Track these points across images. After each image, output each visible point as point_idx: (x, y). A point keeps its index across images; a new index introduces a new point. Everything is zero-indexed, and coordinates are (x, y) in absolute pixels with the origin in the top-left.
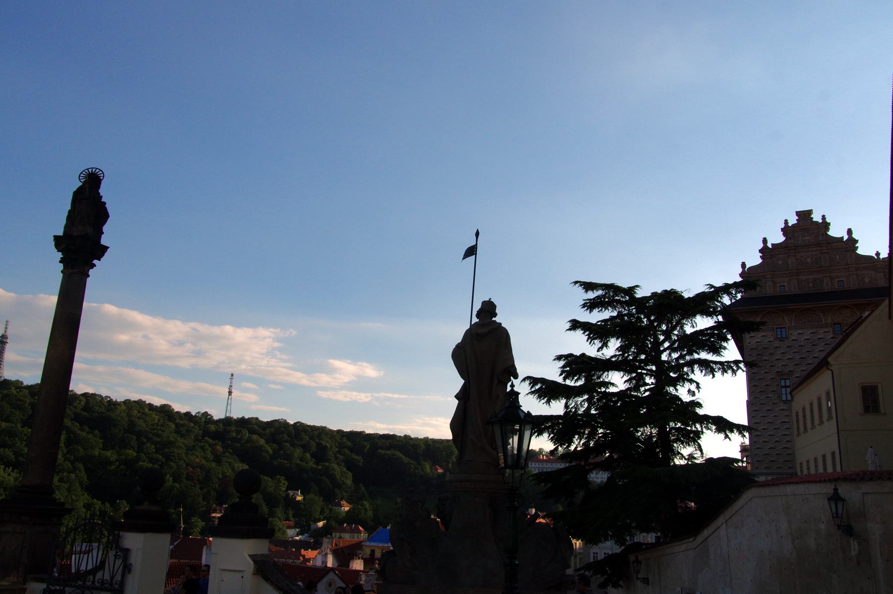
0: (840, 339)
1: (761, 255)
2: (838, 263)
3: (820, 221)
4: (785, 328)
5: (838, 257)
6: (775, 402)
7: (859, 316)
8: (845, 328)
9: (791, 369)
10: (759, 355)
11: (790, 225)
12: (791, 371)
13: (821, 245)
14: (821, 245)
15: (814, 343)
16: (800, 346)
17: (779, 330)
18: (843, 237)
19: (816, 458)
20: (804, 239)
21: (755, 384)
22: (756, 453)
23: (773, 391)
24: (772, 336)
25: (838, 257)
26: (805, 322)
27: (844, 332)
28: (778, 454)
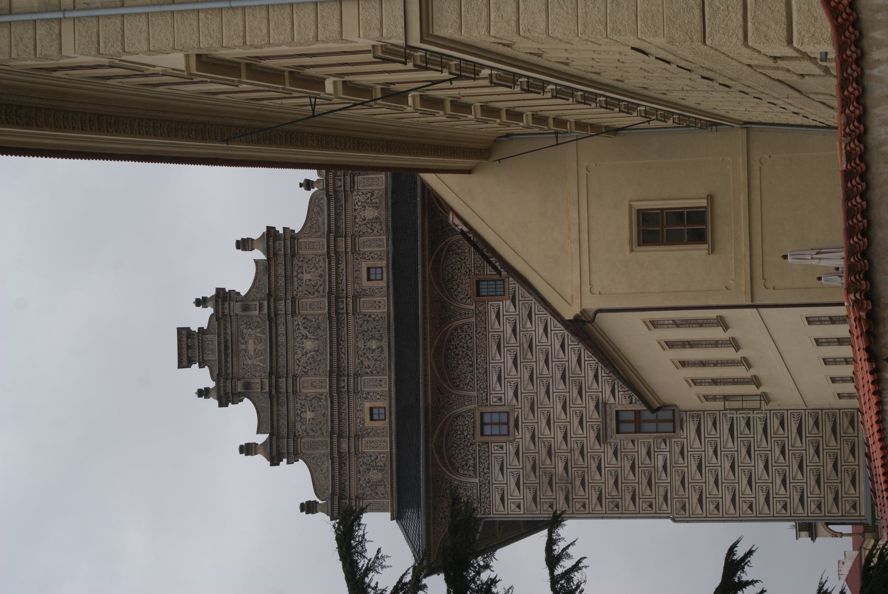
0: (517, 286)
1: (285, 460)
3: (210, 311)
4: (482, 414)
5: (306, 276)
6: (678, 450)
7: (460, 237)
8: (489, 270)
9: (592, 405)
10: (550, 483)
11: (212, 384)
12: (597, 407)
13: (272, 315)
14: (272, 315)
15: (526, 346)
16: (531, 378)
17: (487, 430)
18: (257, 262)
19: (826, 361)
20: (252, 353)
21: (628, 497)
22: (813, 507)
23: (649, 453)
24: (502, 447)
25: (306, 276)
26: (471, 366)
27: (499, 273)
28: (817, 452)
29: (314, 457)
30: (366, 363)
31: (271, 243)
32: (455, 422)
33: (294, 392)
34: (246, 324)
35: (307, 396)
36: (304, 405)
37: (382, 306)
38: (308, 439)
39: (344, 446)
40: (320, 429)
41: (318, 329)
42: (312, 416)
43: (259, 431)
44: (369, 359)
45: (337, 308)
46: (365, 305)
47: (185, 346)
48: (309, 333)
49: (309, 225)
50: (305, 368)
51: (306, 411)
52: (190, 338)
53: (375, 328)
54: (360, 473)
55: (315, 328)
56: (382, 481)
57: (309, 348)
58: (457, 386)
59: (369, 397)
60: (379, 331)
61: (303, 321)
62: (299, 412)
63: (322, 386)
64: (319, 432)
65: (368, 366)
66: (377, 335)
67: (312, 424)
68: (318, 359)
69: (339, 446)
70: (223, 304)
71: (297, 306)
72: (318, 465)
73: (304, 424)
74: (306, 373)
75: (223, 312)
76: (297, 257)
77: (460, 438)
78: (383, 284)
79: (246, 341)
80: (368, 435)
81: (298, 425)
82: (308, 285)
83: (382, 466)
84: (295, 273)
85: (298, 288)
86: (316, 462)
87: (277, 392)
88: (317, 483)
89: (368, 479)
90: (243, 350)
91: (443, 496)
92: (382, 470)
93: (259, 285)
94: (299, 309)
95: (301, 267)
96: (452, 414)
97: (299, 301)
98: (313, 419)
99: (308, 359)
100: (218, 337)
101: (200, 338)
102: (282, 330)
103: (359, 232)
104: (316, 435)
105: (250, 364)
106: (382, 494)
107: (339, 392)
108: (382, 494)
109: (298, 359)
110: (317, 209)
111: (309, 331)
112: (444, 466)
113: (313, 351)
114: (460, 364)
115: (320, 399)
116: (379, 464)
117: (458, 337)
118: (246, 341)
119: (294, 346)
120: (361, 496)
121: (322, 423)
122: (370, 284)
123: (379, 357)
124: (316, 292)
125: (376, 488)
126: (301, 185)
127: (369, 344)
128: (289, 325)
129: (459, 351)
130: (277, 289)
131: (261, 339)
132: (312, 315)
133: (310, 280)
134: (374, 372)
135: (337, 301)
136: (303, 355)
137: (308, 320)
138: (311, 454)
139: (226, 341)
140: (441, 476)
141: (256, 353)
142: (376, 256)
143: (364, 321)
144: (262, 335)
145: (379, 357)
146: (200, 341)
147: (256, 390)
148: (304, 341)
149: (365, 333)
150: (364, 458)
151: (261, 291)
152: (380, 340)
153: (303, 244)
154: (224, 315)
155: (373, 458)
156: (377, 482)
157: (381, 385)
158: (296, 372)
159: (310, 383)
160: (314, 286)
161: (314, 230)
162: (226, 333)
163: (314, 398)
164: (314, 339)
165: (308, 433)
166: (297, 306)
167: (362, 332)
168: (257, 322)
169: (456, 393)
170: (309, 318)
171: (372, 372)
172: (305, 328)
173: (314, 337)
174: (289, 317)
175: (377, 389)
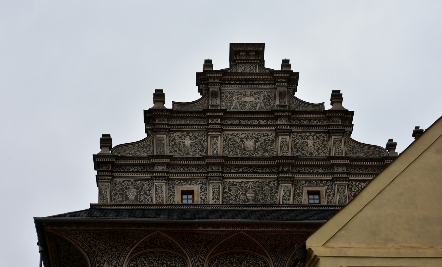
2: (311, 154)
18: (322, 104)
20: (243, 99)
25: (310, 143)
29: (150, 145)
30: (233, 188)
31: (340, 115)
32: (179, 259)
33: (207, 131)
34: (268, 95)
35: (204, 141)
36: (196, 138)
37: (285, 202)
38: (166, 140)
39: (160, 168)
42: (186, 144)
43: (174, 103)
44: (237, 191)
45: (283, 165)
46: (286, 188)
48: (260, 144)
49: (356, 146)
50: (230, 140)
51: (191, 140)
53: (265, 196)
54: (135, 181)
55: (265, 148)
56: (127, 199)
58: (212, 262)
59: (203, 190)
60: (263, 199)
61: (271, 139)
62: (191, 134)
63: (213, 152)
64: (172, 150)
65: (231, 190)
67: (180, 144)
68: (237, 150)
69: (159, 164)
70: (285, 78)
71: (284, 134)
72: (143, 148)
74: (225, 140)
76: (328, 136)
77: (163, 263)
78: (305, 202)
79: (253, 95)
80: (168, 189)
81: (179, 134)
82: (303, 143)
83: (140, 199)
84: (313, 134)
85: (300, 136)
87: (209, 117)
88: (127, 147)
89: (129, 188)
90: (245, 93)
91: (110, 245)
92: (136, 199)
93: (302, 107)
95: (319, 138)
96: (186, 257)
97: (288, 135)
98: (184, 145)
99: (237, 143)
100: (257, 73)
101: (255, 61)
102: (263, 122)
103: (351, 185)
105: (234, 98)
106: (114, 199)
107: (208, 165)
108: (114, 199)
109: (237, 134)
110: (370, 152)
111: (262, 143)
112: (138, 246)
113: (244, 147)
114: (232, 265)
115: (202, 151)
116: (142, 197)
117: (258, 264)
118: (253, 95)
119: (249, 132)
120: (114, 181)
121: (180, 152)
122: (305, 193)
123: (240, 199)
124: (297, 149)
125: (120, 194)
126: (391, 140)
127: (251, 191)
128: (268, 128)
129: (245, 265)
130: (299, 119)
132: (276, 147)
133: (307, 145)
134: (225, 195)
136: (241, 138)
138: (153, 143)
139: (252, 80)
140: (129, 242)
141: (243, 103)
142: (331, 198)
143: (271, 187)
144: (258, 107)
145: (240, 199)
146: (253, 61)
147: (210, 101)
148: (254, 140)
149: (261, 187)
150: (148, 185)
151: (297, 108)
152: (254, 201)
154: (275, 78)
155: (148, 192)
156: (126, 195)
157: (213, 199)
158: (226, 133)
160: (302, 149)
161: (351, 149)
162: (260, 80)
164: (255, 147)
165: (172, 141)
166: (284, 134)
167: (262, 186)
168: (270, 104)
169: (206, 260)
170: (274, 144)
171: (225, 193)
172: (265, 141)
173: (257, 148)
174: (274, 128)
175: (210, 196)
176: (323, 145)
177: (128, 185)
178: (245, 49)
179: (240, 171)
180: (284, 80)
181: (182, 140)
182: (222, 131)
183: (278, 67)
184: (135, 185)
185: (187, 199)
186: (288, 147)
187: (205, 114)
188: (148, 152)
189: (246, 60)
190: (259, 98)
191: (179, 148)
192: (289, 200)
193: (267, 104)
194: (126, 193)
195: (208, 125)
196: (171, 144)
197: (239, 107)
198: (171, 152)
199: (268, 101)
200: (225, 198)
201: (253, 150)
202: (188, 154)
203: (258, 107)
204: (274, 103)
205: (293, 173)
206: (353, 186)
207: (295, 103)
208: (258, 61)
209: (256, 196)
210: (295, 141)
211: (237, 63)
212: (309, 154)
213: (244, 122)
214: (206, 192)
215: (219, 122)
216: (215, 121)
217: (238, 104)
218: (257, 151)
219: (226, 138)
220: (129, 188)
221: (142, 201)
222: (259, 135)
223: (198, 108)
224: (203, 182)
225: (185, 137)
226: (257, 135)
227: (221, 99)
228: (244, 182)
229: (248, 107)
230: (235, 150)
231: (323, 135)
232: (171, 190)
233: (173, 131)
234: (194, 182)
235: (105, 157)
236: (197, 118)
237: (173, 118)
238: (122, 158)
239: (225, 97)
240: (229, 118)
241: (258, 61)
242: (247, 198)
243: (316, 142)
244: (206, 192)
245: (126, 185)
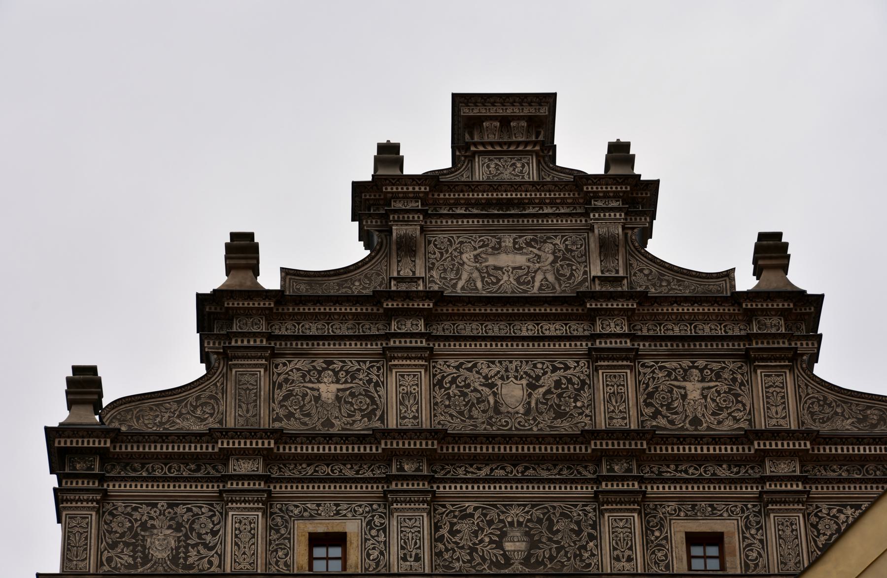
2: (696, 421)
5: (694, 389)
18: (729, 275)
20: (491, 261)
25: (694, 389)
29: (216, 399)
30: (464, 527)
31: (781, 305)
33: (387, 355)
34: (566, 249)
35: (377, 385)
36: (353, 378)
37: (618, 565)
38: (264, 384)
39: (245, 467)
40: (290, 415)
41: (555, 412)
43: (286, 273)
44: (476, 533)
45: (613, 456)
46: (621, 524)
47: (509, 112)
48: (545, 394)
49: (831, 397)
50: (453, 381)
51: (338, 382)
52: (528, 126)
53: (559, 550)
54: (170, 506)
55: (559, 406)
56: (146, 559)
57: (504, 391)
59: (374, 532)
60: (551, 558)
61: (575, 380)
62: (337, 366)
63: (404, 418)
65: (459, 532)
66: (542, 553)
67: (305, 395)
68: (475, 413)
69: (244, 454)
70: (616, 196)
71: (615, 363)
72: (196, 407)
73: (304, 376)
74: (440, 384)
75: (596, 196)
76: (745, 368)
79: (521, 248)
80: (269, 529)
81: (302, 364)
82: (671, 392)
83: (186, 559)
84: (701, 363)
85: (661, 368)
86: (202, 405)
87: (390, 315)
88: (146, 405)
89: (153, 527)
90: (499, 243)
92: (175, 559)
93: (669, 283)
94: (608, 367)
97: (627, 367)
98: (317, 398)
99: (475, 390)
100: (533, 184)
101: (529, 148)
102: (552, 329)
103: (816, 515)
104: (275, 406)
105: (464, 257)
106: (109, 560)
107: (388, 457)
108: (109, 560)
109: (475, 365)
110: (873, 415)
111: (549, 392)
113: (496, 402)
115: (370, 415)
116: (193, 552)
118: (521, 248)
119: (510, 357)
120: (109, 507)
123: (483, 558)
124: (653, 410)
125: (127, 545)
127: (517, 533)
130: (657, 319)
131: (528, 283)
132: (592, 404)
133: (684, 397)
135: (630, 455)
137: (578, 390)
138: (224, 392)
139: (520, 204)
141: (491, 272)
142: (755, 555)
143: (578, 523)
144: (537, 284)
145: (483, 558)
147: (394, 267)
148: (524, 382)
149: (546, 523)
150: (210, 517)
151: (654, 285)
152: (526, 561)
153: (780, 379)
154: (588, 198)
155: (208, 538)
156: (144, 547)
157: (404, 559)
158: (441, 362)
159: (414, 390)
160: (669, 407)
161: (816, 408)
162: (542, 203)
163: (373, 401)
164: (529, 403)
165: (280, 387)
166: (615, 363)
167: (549, 519)
168: (572, 275)
170: (586, 394)
171: (441, 539)
172: (558, 384)
173: (533, 404)
174: (583, 346)
175: (394, 549)
176: (731, 397)
177: (152, 518)
178: (499, 111)
179: (482, 473)
180: (614, 204)
181: (310, 381)
182: (431, 356)
183: (594, 165)
184: (172, 519)
185: (327, 559)
186: (625, 401)
187: (379, 304)
188: (211, 420)
189: (500, 144)
190: (539, 257)
191: (301, 408)
192: (629, 559)
193: (564, 275)
194: (144, 540)
195: (388, 337)
196: (279, 394)
197: (479, 285)
198: (278, 419)
199: (568, 265)
200: (439, 554)
201: (522, 411)
202: (328, 423)
203: (537, 284)
204: (585, 273)
205: (641, 480)
206: (820, 518)
207: (646, 272)
208: (537, 148)
209: (530, 549)
210: (648, 385)
211: (475, 153)
212: (691, 423)
213: (495, 329)
214: (382, 538)
215: (421, 327)
216: (408, 326)
217: (476, 274)
218: (534, 413)
219: (443, 377)
220: (153, 527)
221: (191, 566)
222: (539, 366)
223: (357, 288)
224: (375, 507)
225: (320, 372)
226: (535, 366)
227: (426, 260)
228: (495, 506)
229: (508, 285)
230: (470, 411)
231: (731, 366)
232: (278, 531)
233: (282, 355)
234: (346, 506)
235: (81, 434)
236: (356, 316)
237: (283, 317)
238: (132, 436)
239: (438, 255)
240: (450, 317)
241: (537, 148)
242: (504, 555)
243: (710, 388)
244: (382, 538)
245: (145, 518)
